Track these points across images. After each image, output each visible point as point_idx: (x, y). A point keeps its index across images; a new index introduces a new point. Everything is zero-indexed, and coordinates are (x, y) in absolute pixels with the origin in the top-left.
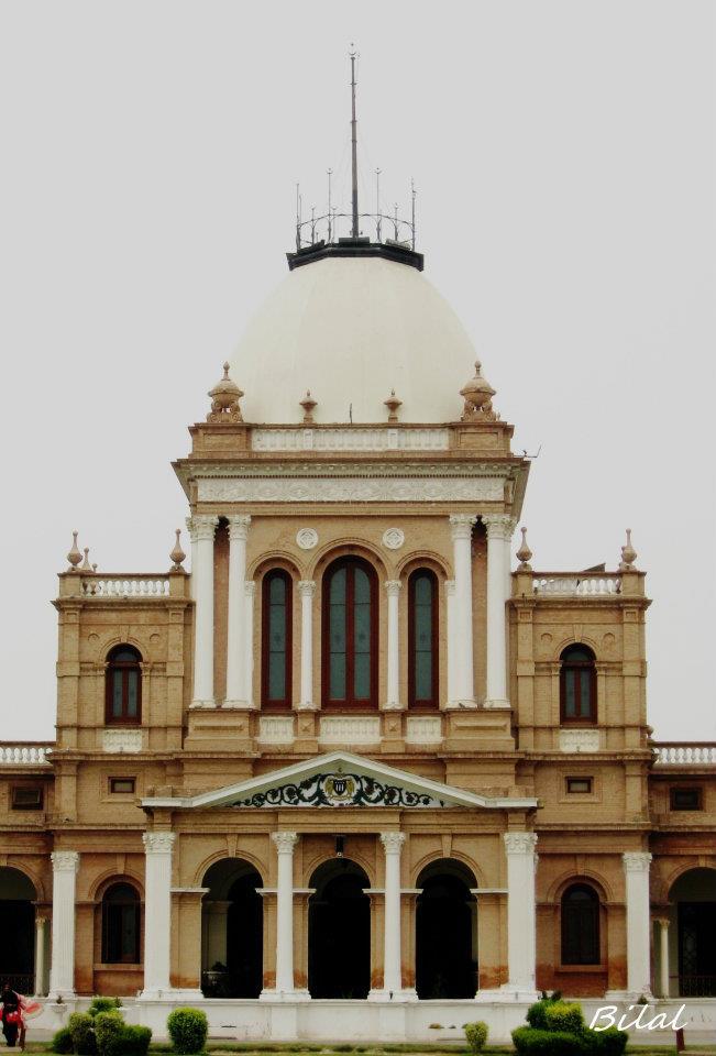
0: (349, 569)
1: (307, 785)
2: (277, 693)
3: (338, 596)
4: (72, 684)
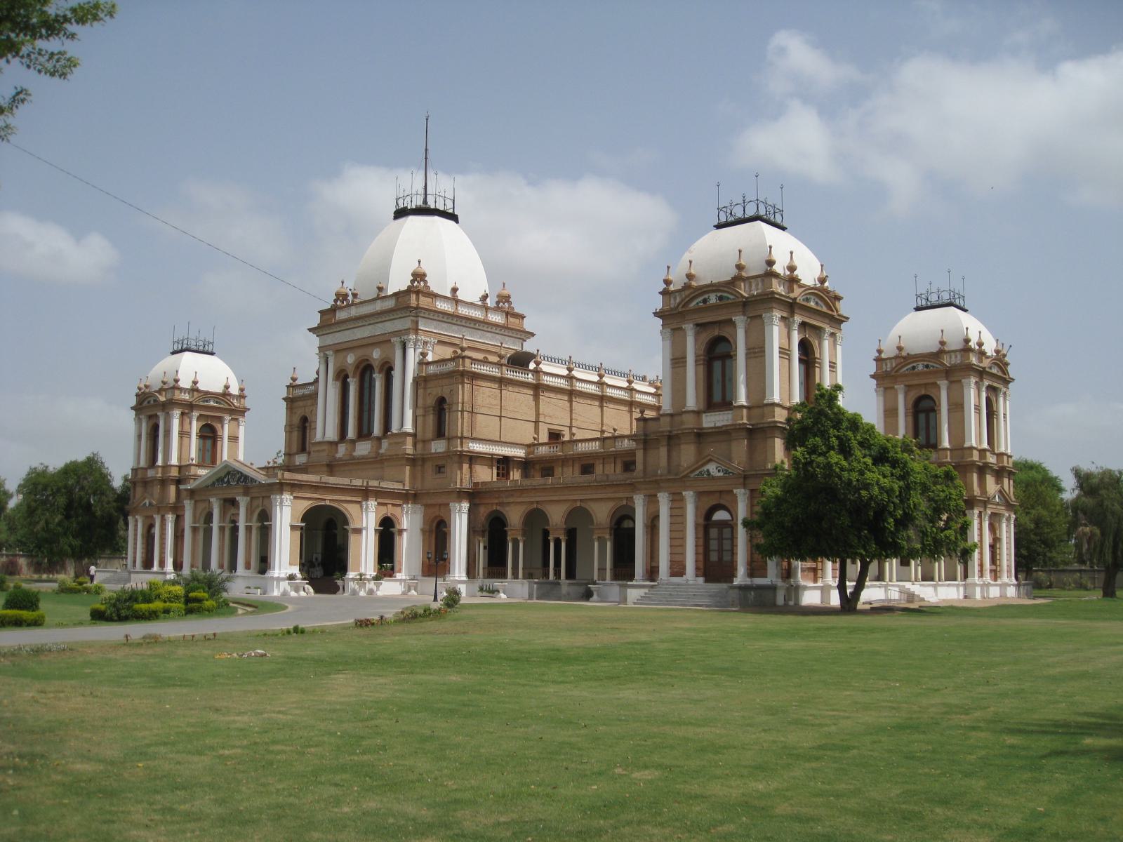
0: (365, 369)
1: (225, 477)
2: (365, 431)
3: (366, 385)
4: (288, 433)
